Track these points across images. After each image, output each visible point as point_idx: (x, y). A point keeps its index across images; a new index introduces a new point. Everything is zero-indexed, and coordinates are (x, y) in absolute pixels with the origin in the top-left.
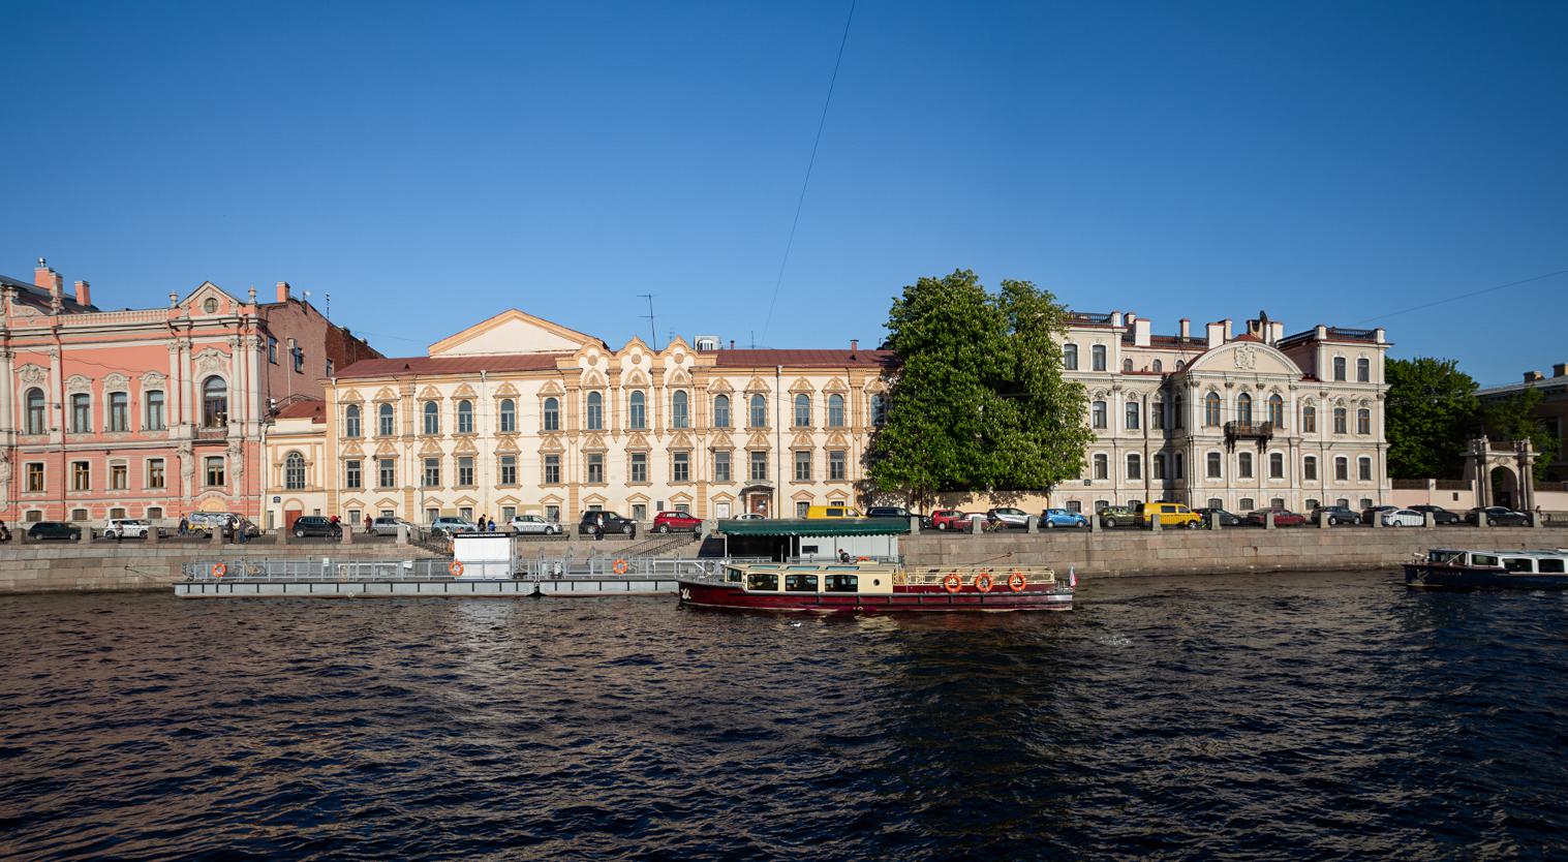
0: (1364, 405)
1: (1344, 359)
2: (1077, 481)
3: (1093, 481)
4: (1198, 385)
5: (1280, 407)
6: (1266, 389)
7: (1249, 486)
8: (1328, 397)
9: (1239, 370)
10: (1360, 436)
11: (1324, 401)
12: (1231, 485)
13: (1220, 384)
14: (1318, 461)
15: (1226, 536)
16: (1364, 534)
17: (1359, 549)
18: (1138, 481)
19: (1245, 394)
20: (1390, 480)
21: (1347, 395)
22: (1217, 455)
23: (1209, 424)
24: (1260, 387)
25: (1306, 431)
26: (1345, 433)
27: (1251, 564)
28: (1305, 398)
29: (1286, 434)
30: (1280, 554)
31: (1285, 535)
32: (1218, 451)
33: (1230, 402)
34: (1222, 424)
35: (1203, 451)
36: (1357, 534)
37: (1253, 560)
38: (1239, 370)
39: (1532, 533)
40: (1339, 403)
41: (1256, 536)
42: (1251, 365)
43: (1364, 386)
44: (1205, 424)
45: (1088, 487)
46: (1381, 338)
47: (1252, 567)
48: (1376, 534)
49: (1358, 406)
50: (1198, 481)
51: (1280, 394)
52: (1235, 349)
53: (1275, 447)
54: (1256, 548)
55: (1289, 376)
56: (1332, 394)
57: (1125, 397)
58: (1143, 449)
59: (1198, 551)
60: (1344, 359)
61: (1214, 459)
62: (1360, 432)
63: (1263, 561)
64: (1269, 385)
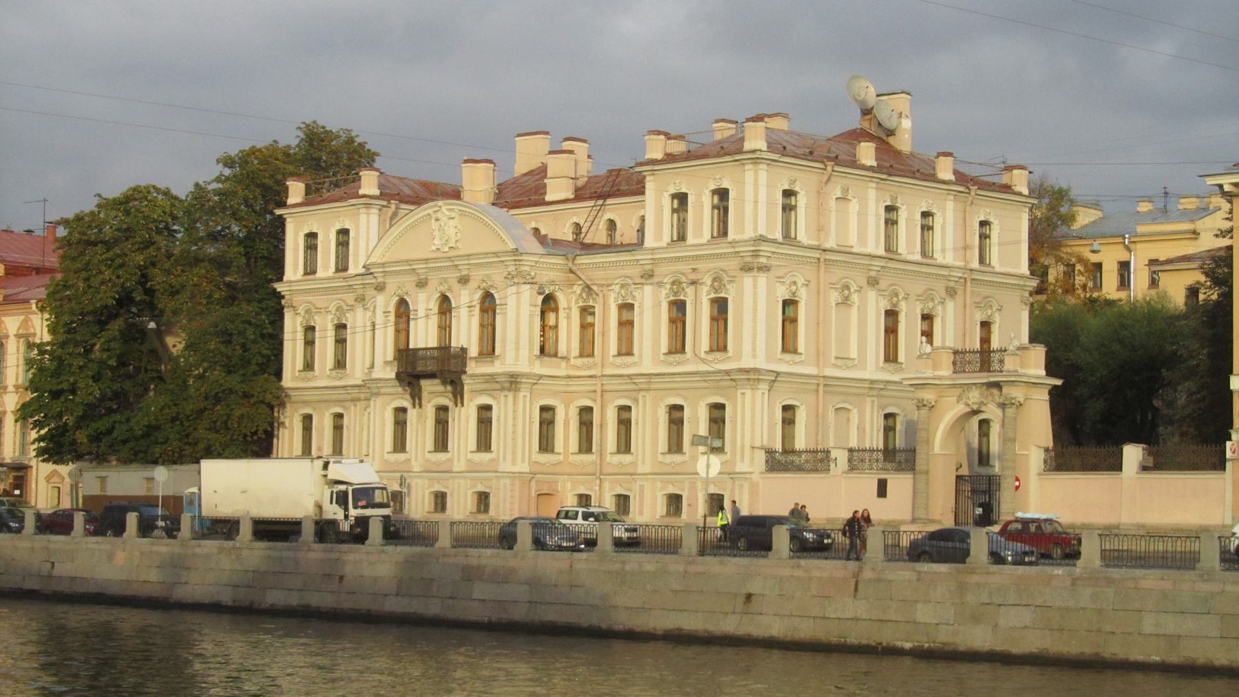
6: (473, 284)
8: (656, 280)
11: (648, 289)
22: (404, 410)
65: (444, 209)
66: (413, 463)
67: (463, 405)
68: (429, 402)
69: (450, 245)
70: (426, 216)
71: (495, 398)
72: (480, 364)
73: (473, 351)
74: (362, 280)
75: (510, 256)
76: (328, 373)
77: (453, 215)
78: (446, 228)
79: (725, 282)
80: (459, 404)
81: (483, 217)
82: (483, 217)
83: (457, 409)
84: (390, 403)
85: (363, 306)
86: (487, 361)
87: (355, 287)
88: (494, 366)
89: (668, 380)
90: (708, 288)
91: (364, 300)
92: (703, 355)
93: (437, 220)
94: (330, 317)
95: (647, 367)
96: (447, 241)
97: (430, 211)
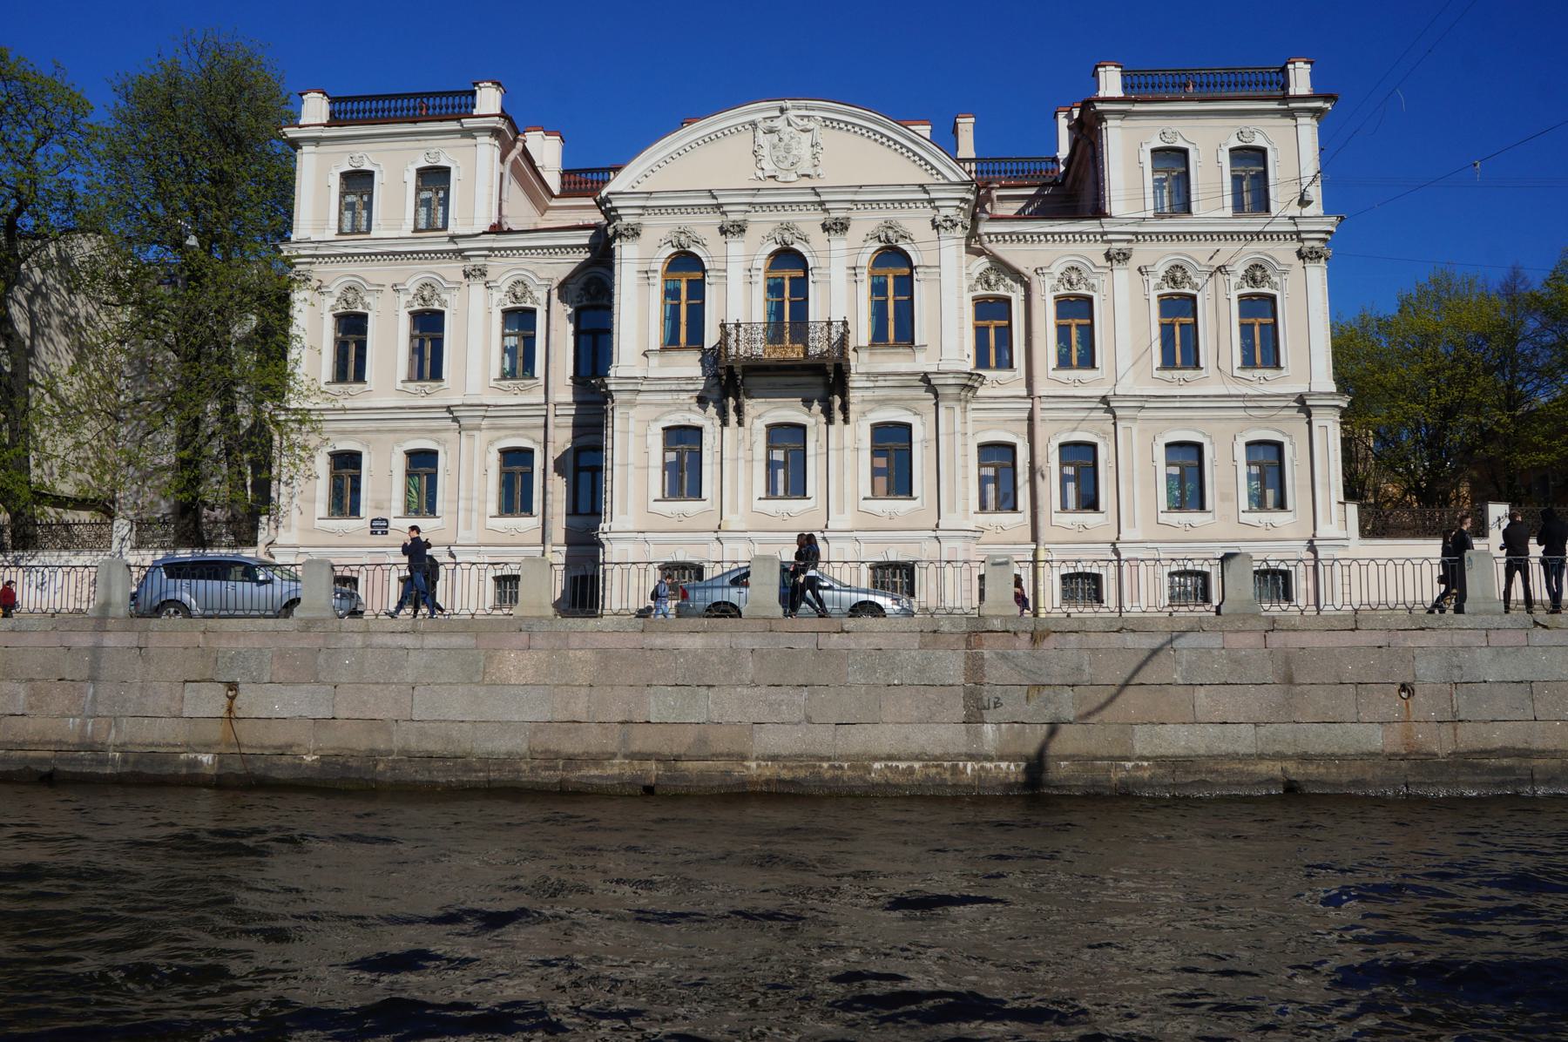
1: (1185, 152)
4: (634, 232)
5: (906, 285)
8: (1135, 262)
9: (771, 183)
10: (1248, 374)
11: (1123, 276)
12: (732, 520)
13: (704, 228)
14: (1104, 454)
15: (131, 639)
17: (660, 705)
20: (1353, 508)
21: (1199, 253)
23: (671, 343)
24: (837, 227)
25: (1064, 362)
26: (1197, 366)
27: (207, 747)
28: (1057, 269)
29: (922, 362)
30: (324, 712)
31: (358, 641)
33: (736, 274)
36: (659, 641)
37: (216, 732)
38: (771, 183)
39: (1458, 639)
40: (1171, 277)
41: (242, 644)
43: (1255, 224)
45: (379, 539)
46: (1301, 79)
47: (206, 758)
48: (747, 642)
49: (1233, 289)
50: (624, 512)
51: (902, 245)
52: (754, 124)
53: (883, 402)
54: (232, 686)
56: (1142, 253)
57: (497, 295)
58: (540, 435)
59: (22, 691)
60: (1185, 152)
61: (683, 439)
62: (1248, 362)
63: (253, 737)
64: (865, 224)
65: (791, 114)
67: (846, 421)
68: (759, 416)
72: (878, 358)
73: (862, 333)
76: (400, 386)
77: (811, 125)
78: (794, 143)
80: (838, 416)
86: (898, 353)
89: (1178, 405)
90: (1239, 280)
91: (484, 274)
92: (1237, 373)
93: (771, 131)
94: (404, 298)
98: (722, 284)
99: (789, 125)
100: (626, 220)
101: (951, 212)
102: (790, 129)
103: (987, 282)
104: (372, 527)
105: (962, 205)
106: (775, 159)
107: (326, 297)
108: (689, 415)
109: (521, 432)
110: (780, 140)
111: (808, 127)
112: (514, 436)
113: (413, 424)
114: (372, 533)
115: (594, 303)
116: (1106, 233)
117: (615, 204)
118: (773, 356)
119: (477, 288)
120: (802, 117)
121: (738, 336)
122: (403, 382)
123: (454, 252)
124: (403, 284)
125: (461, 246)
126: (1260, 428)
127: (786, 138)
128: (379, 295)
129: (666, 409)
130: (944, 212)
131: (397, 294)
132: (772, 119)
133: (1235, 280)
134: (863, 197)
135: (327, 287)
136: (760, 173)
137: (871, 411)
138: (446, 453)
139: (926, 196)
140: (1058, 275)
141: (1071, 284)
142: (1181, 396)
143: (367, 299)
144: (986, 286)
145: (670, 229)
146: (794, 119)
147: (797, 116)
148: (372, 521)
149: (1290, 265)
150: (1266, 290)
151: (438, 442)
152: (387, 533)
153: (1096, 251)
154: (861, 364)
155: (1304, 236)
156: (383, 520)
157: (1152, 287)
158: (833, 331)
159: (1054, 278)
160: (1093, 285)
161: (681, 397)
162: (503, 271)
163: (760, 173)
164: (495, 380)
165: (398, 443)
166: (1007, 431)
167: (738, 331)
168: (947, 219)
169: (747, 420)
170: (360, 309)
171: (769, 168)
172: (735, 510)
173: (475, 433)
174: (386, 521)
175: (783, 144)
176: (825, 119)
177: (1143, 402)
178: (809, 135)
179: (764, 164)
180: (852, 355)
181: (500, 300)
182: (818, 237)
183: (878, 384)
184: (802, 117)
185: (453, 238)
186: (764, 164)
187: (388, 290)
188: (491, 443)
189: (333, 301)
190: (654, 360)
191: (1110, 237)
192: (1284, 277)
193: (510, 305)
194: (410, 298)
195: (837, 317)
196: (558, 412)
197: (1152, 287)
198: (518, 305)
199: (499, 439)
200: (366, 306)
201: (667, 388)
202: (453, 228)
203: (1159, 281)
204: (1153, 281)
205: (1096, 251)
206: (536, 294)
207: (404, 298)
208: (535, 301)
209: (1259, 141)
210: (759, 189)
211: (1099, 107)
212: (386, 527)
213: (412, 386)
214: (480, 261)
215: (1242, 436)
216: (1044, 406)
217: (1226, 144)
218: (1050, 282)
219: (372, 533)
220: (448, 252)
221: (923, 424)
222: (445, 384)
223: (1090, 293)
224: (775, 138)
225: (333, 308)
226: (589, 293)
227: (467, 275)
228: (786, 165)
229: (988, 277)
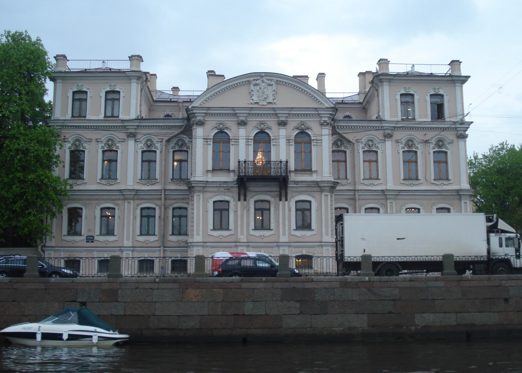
0: (440, 147)
2: (77, 238)
3: (96, 238)
4: (201, 124)
7: (265, 240)
11: (389, 144)
16: (261, 285)
18: (152, 238)
19: (262, 132)
21: (419, 136)
24: (283, 124)
28: (364, 140)
29: (314, 178)
32: (227, 198)
33: (242, 143)
34: (233, 165)
35: (205, 202)
42: (270, 100)
44: (210, 168)
49: (431, 149)
50: (198, 234)
53: (301, 193)
55: (316, 109)
56: (398, 135)
57: (141, 145)
64: (293, 123)
65: (264, 79)
66: (239, 236)
67: (286, 200)
68: (252, 197)
69: (268, 101)
70: (248, 81)
71: (313, 197)
74: (139, 123)
75: (327, 111)
77: (272, 83)
78: (265, 90)
79: (445, 143)
81: (300, 86)
82: (300, 86)
83: (281, 203)
84: (212, 198)
85: (135, 140)
87: (127, 127)
88: (312, 177)
93: (256, 85)
94: (101, 145)
95: (391, 186)
96: (265, 98)
97: (251, 79)
98: (237, 145)
99: (263, 82)
100: (198, 118)
101: (326, 119)
102: (263, 84)
103: (337, 145)
104: (87, 239)
105: (331, 116)
106: (258, 96)
107: (67, 143)
108: (224, 197)
109: (150, 201)
110: (260, 88)
111: (271, 83)
112: (147, 203)
113: (104, 197)
114: (87, 242)
115: (181, 149)
116: (383, 126)
117: (194, 111)
118: (259, 174)
119: (131, 143)
120: (268, 80)
121: (245, 166)
122: (100, 179)
123: (122, 126)
124: (100, 139)
125: (125, 124)
126: (441, 203)
127: (262, 88)
128: (90, 143)
129: (215, 194)
130: (324, 119)
131: (97, 143)
132: (257, 80)
133: (432, 146)
134: (292, 112)
135: (67, 139)
136: (251, 101)
137: (296, 195)
138: (118, 209)
139: (316, 113)
140: (364, 142)
141: (369, 146)
142: (412, 190)
143: (85, 145)
144: (337, 147)
145: (216, 122)
146: (265, 80)
147: (266, 79)
148: (87, 237)
149: (453, 140)
150: (444, 150)
151: (115, 204)
152: (93, 242)
153: (379, 135)
154: (293, 177)
155: (458, 129)
156: (92, 236)
157: (400, 148)
158: (282, 165)
159: (363, 144)
160: (378, 147)
161: (221, 189)
162: (143, 135)
163: (251, 101)
164: (139, 179)
165: (98, 204)
166: (345, 203)
167: (245, 164)
168: (325, 121)
169: (247, 198)
170: (81, 149)
171: (255, 99)
172: (242, 234)
173: (132, 201)
174: (93, 237)
175: (261, 90)
176: (277, 81)
177: (398, 193)
178: (271, 87)
179: (253, 98)
180: (289, 174)
181: (141, 146)
182: (275, 127)
183: (298, 185)
184: (268, 80)
185: (123, 121)
186: (253, 98)
187: (94, 142)
188: (138, 205)
189: (70, 145)
190: (210, 175)
191: (384, 128)
192: (450, 145)
193: (145, 149)
194: (103, 145)
195: (283, 158)
196: (166, 193)
197: (400, 148)
198: (149, 149)
199: (141, 204)
200: (84, 148)
201: (215, 185)
202: (121, 117)
203: (403, 145)
204: (401, 146)
205: (379, 135)
206: (156, 145)
207: (101, 145)
208: (156, 148)
209: (441, 92)
210: (252, 108)
211: (381, 77)
212: (93, 239)
213: (104, 182)
214: (133, 131)
215: (435, 206)
216: (359, 194)
217: (429, 93)
218: (361, 146)
219: (87, 242)
220: (119, 126)
221: (316, 201)
222: (118, 181)
223: (377, 150)
224: (258, 88)
225: (70, 148)
226: (178, 145)
227: (128, 136)
228: (262, 98)
229: (337, 143)
